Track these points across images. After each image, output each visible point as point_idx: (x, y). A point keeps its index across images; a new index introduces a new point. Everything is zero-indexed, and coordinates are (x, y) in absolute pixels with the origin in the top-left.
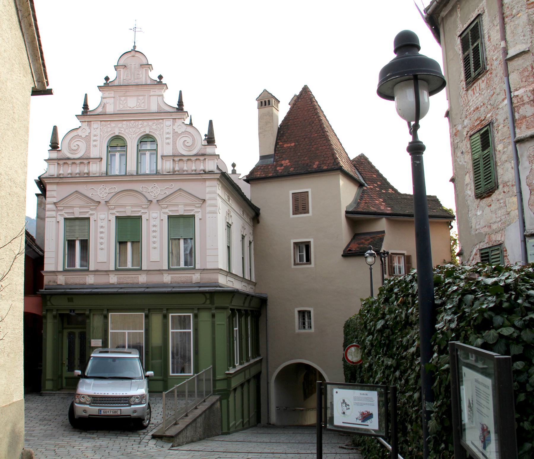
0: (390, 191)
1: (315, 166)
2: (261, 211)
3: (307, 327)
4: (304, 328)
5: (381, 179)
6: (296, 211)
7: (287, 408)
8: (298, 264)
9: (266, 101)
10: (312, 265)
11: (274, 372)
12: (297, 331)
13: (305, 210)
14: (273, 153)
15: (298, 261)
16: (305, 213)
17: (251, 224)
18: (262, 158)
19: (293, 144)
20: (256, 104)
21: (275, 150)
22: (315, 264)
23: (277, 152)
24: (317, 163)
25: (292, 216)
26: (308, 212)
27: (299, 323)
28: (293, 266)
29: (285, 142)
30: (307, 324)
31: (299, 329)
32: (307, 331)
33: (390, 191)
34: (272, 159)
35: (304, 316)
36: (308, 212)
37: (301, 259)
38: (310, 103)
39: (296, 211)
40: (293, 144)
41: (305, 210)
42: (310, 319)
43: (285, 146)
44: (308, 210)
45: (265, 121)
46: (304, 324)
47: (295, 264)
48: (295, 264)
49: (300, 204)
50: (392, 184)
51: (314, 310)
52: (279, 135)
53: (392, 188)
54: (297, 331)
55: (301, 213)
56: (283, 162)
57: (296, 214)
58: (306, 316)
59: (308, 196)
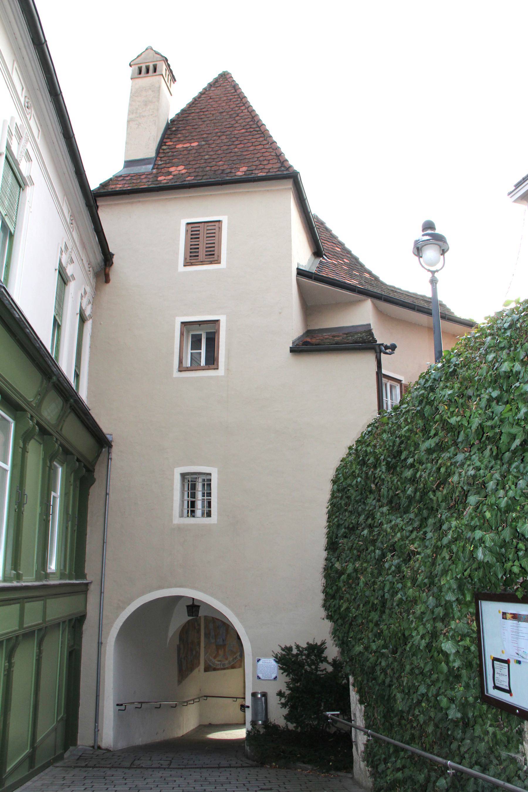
0: (367, 275)
1: (239, 174)
2: (115, 259)
3: (199, 512)
4: (193, 513)
5: (349, 256)
6: (193, 257)
7: (141, 703)
8: (187, 369)
9: (149, 67)
10: (221, 371)
11: (117, 616)
12: (177, 520)
13: (212, 256)
14: (151, 153)
15: (188, 363)
16: (211, 263)
17: (94, 283)
18: (129, 164)
19: (195, 144)
20: (129, 71)
21: (158, 152)
22: (227, 370)
23: (161, 155)
24: (244, 169)
25: (181, 268)
26: (218, 261)
27: (183, 502)
28: (176, 374)
29: (179, 141)
30: (199, 504)
31: (182, 516)
32: (199, 520)
33: (367, 275)
34: (151, 166)
35: (193, 487)
36: (218, 261)
37: (195, 359)
38: (233, 91)
39: (193, 257)
40: (195, 144)
41: (212, 256)
42: (209, 494)
43: (179, 146)
44: (219, 256)
45: (141, 105)
46: (193, 504)
47: (181, 369)
48: (181, 369)
49: (202, 246)
50: (368, 266)
51: (219, 473)
52: (169, 132)
53: (370, 273)
54: (177, 520)
55: (202, 263)
56: (172, 169)
57: (192, 264)
58: (199, 487)
59: (220, 228)
